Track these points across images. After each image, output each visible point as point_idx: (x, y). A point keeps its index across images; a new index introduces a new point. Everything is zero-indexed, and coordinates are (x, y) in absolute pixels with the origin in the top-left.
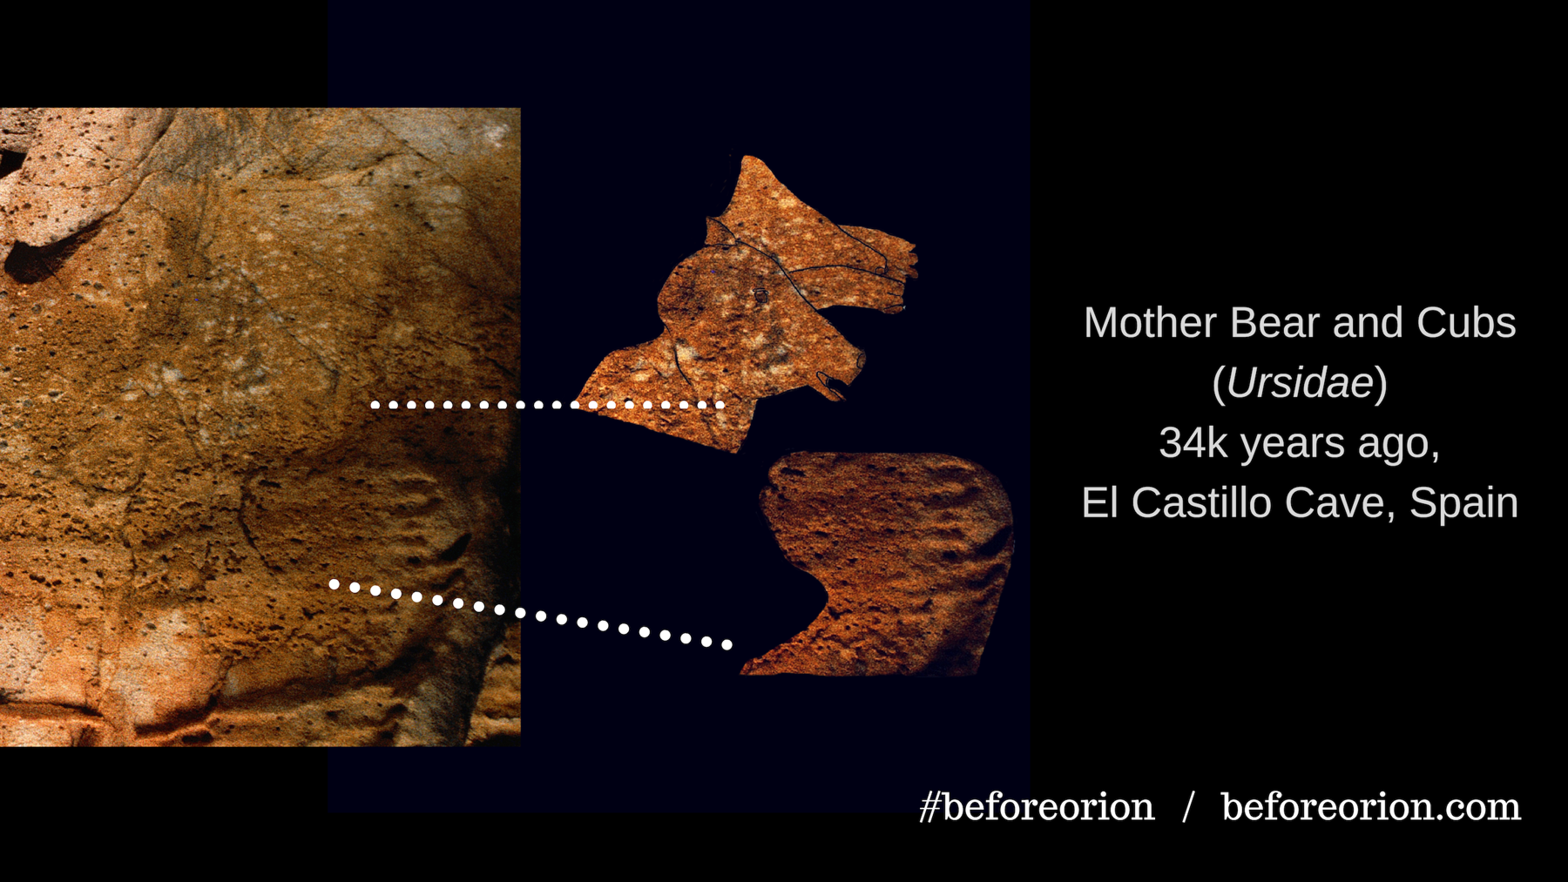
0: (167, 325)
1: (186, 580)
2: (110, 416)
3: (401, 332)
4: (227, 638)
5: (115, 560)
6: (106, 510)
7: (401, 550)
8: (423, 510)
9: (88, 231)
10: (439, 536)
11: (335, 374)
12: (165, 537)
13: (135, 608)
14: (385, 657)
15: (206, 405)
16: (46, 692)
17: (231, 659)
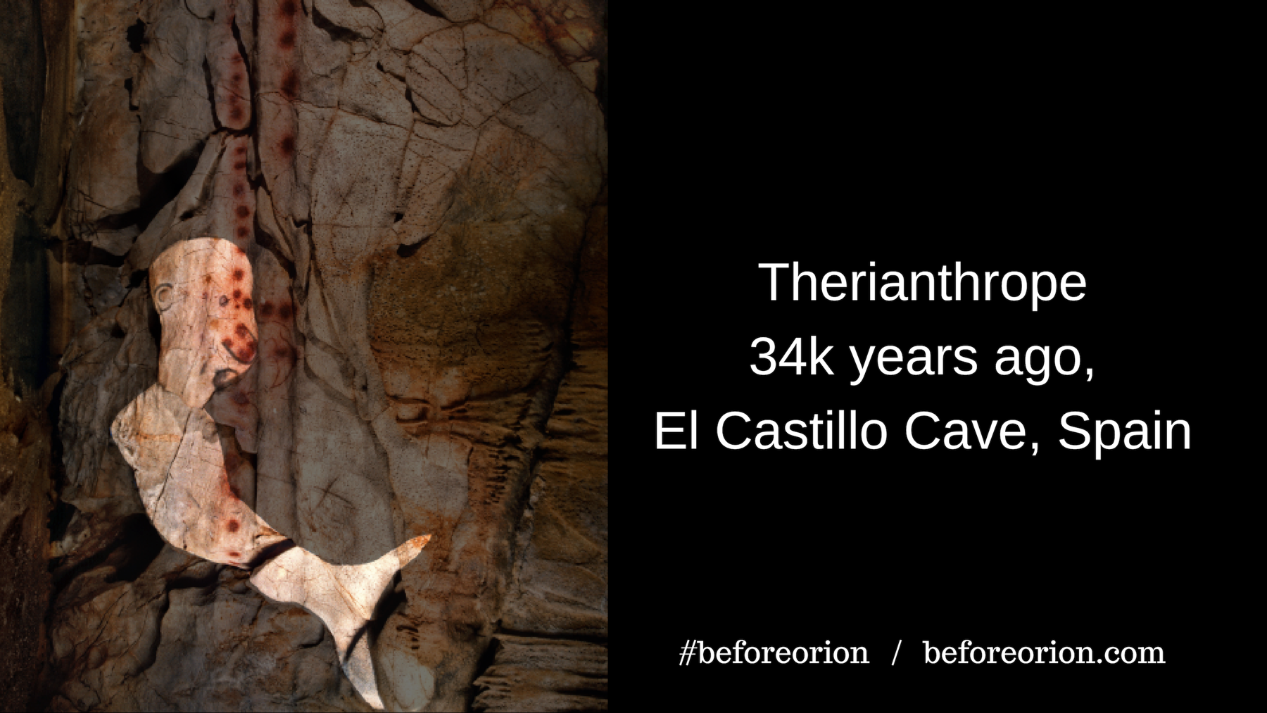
0: (452, 272)
1: (458, 358)
2: (432, 302)
3: (531, 274)
4: (472, 377)
5: (434, 351)
6: (431, 334)
7: (530, 348)
8: (538, 334)
9: (425, 240)
10: (543, 342)
11: (508, 288)
12: (451, 343)
13: (441, 367)
14: (525, 383)
15: (465, 298)
16: (411, 395)
17: (473, 384)
